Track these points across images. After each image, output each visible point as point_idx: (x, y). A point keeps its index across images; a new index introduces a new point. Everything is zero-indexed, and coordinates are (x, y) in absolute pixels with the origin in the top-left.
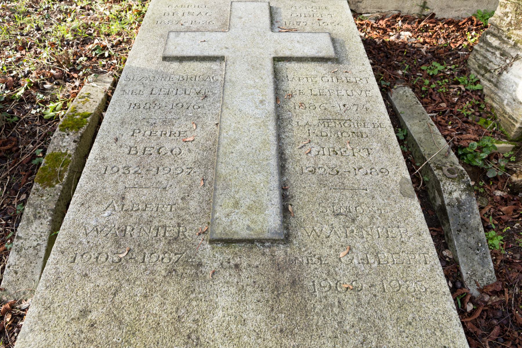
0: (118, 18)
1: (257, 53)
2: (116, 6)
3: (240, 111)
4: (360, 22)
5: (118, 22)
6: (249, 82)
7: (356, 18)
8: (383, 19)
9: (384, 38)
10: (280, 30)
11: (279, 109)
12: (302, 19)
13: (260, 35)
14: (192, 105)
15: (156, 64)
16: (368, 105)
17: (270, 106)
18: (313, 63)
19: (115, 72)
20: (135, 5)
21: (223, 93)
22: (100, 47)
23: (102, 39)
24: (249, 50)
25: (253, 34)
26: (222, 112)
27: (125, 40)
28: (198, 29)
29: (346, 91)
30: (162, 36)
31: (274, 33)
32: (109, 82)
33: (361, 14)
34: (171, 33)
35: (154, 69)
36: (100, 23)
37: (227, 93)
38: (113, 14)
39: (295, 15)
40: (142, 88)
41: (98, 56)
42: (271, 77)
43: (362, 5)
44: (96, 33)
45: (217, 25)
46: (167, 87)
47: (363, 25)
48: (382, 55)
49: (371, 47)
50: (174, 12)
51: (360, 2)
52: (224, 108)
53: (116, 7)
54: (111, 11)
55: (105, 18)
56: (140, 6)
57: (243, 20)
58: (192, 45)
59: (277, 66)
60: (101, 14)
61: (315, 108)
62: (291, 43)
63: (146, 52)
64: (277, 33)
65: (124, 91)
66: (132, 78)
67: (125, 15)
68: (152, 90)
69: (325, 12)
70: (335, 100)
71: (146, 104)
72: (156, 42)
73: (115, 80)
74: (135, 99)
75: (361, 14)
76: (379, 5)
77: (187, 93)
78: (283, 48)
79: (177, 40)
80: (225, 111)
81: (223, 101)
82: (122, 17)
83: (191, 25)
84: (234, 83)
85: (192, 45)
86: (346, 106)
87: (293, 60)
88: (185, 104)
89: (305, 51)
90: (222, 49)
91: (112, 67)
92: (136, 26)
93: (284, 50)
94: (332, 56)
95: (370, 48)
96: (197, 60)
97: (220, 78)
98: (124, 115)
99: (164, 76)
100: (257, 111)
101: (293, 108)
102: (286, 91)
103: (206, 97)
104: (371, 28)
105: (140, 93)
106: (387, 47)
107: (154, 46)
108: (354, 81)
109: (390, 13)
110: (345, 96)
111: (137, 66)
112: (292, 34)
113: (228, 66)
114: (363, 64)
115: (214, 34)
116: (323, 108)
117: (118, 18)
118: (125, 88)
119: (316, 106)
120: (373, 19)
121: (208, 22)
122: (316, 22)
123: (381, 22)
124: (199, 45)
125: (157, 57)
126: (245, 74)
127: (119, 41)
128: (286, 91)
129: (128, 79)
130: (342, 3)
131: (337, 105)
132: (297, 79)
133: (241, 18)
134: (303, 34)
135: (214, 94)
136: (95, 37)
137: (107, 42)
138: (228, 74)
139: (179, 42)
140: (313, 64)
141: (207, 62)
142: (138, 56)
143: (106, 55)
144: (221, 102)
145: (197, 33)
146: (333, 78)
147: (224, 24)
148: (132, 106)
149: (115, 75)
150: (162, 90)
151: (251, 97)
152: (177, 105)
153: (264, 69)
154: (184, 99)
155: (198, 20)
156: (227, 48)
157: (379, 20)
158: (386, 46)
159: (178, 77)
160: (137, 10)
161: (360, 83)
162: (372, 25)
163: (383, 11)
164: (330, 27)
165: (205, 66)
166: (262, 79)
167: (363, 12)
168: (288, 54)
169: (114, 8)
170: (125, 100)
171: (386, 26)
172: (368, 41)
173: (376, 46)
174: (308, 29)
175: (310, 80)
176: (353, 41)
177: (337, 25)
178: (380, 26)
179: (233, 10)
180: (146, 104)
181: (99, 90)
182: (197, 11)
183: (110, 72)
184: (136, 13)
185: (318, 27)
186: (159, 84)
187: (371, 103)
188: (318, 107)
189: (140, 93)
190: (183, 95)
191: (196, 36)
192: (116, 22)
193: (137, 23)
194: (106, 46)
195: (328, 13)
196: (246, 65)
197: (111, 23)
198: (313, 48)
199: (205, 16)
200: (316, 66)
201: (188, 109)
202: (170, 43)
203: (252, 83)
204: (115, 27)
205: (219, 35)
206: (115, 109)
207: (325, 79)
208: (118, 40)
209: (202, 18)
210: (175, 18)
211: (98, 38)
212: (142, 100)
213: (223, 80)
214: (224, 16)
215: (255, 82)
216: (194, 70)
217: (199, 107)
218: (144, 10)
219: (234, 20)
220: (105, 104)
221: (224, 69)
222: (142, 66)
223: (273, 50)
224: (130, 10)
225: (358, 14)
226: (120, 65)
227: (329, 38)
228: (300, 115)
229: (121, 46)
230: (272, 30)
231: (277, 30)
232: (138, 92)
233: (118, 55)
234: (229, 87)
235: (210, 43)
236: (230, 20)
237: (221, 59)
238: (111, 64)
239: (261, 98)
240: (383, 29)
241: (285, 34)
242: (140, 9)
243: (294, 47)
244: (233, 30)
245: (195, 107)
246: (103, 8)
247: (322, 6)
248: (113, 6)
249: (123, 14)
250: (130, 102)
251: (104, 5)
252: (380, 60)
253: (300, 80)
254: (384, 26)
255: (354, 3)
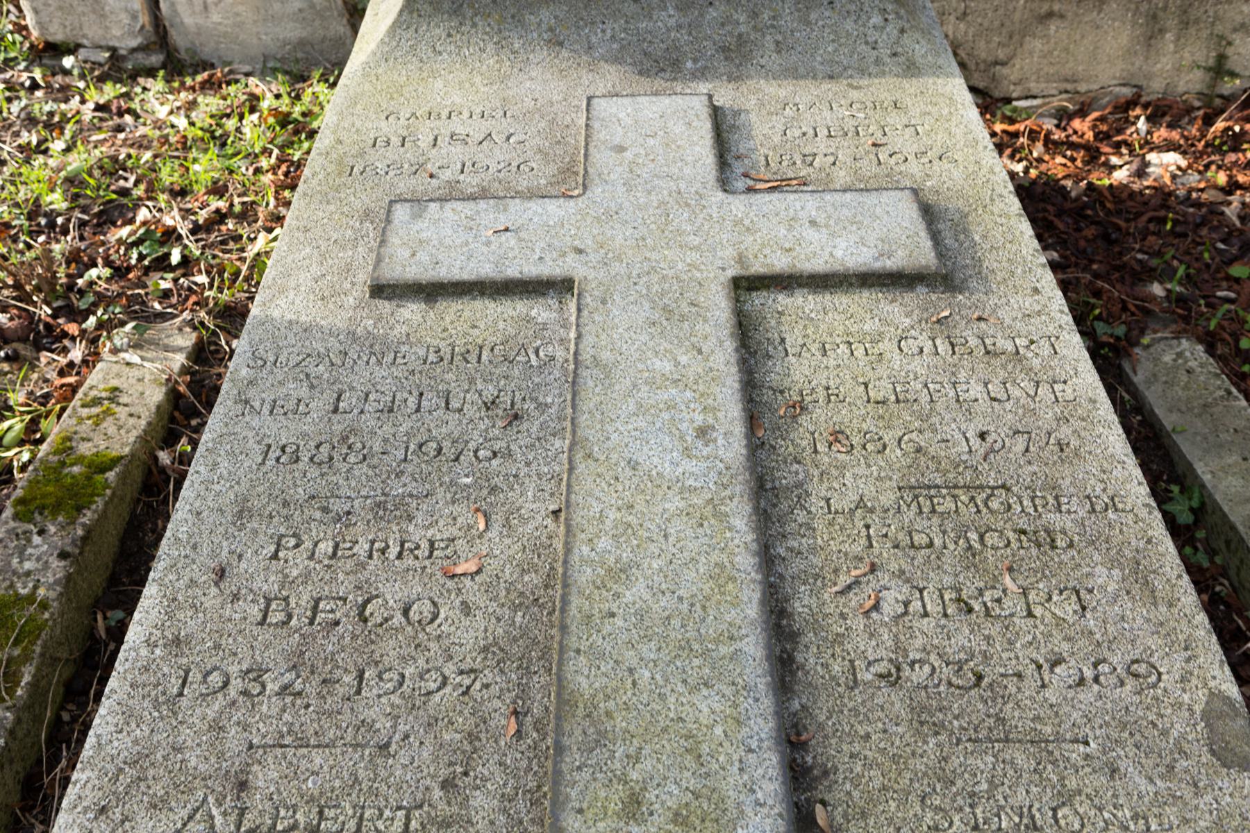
0: (214, 138)
1: (680, 265)
2: (210, 99)
3: (634, 465)
4: (1005, 127)
5: (214, 150)
6: (658, 364)
7: (993, 115)
8: (1082, 113)
9: (1093, 178)
10: (751, 183)
11: (762, 454)
12: (822, 145)
13: (688, 205)
14: (472, 445)
15: (348, 309)
16: (1065, 432)
18: (866, 294)
19: (202, 314)
20: (269, 95)
21: (574, 407)
22: (154, 232)
23: (163, 205)
24: (654, 256)
25: (662, 203)
26: (571, 469)
27: (238, 208)
28: (484, 189)
29: (986, 384)
30: (367, 214)
31: (731, 197)
32: (180, 349)
33: (1008, 101)
34: (398, 206)
36: (155, 156)
38: (199, 125)
39: (797, 133)
40: (304, 392)
41: (146, 263)
42: (730, 345)
43: (1010, 73)
44: (142, 187)
45: (542, 173)
46: (388, 387)
47: (1016, 135)
48: (1090, 232)
49: (1050, 208)
50: (405, 133)
51: (1003, 64)
52: (579, 457)
53: (210, 103)
54: (193, 114)
55: (173, 139)
56: (286, 100)
57: (628, 155)
59: (747, 307)
60: (158, 124)
62: (791, 228)
63: (316, 270)
64: (743, 197)
65: (247, 402)
66: (272, 359)
67: (238, 130)
68: (338, 399)
69: (894, 119)
71: (317, 447)
73: (200, 341)
74: (282, 431)
75: (1008, 101)
76: (1067, 71)
77: (455, 404)
78: (763, 245)
79: (416, 228)
80: (581, 468)
81: (574, 432)
82: (226, 135)
83: (461, 178)
84: (607, 370)
85: (467, 243)
86: (989, 439)
87: (800, 286)
88: (446, 444)
89: (839, 253)
90: (564, 254)
91: (193, 299)
92: (273, 160)
93: (767, 251)
94: (927, 267)
95: (1045, 210)
96: (482, 294)
97: (560, 354)
98: (245, 484)
99: (379, 349)
100: (688, 466)
101: (809, 450)
102: (782, 392)
103: (516, 417)
104: (1045, 145)
105: (298, 410)
106: (1104, 206)
107: (343, 248)
108: (1010, 347)
109: (1105, 95)
110: (984, 405)
111: (289, 316)
112: (792, 196)
113: (585, 313)
115: (535, 206)
116: (910, 448)
117: (214, 138)
118: (251, 393)
119: (886, 439)
120: (1051, 116)
121: (515, 164)
122: (867, 153)
123: (1077, 124)
124: (488, 244)
125: (353, 284)
126: (644, 337)
127: (218, 211)
128: (782, 392)
129: (257, 361)
130: (949, 88)
131: (957, 436)
132: (814, 348)
134: (828, 197)
136: (140, 199)
137: (178, 218)
138: (588, 340)
139: (424, 235)
140: (866, 296)
141: (516, 298)
142: (292, 284)
143: (175, 258)
144: (568, 435)
145: (482, 204)
146: (938, 342)
147: (568, 171)
148: (273, 454)
149: (202, 323)
150: (371, 397)
151: (666, 416)
152: (421, 446)
153: (706, 321)
154: (445, 427)
155: (482, 160)
156: (580, 251)
157: (1071, 117)
158: (1102, 205)
159: (422, 352)
160: (274, 112)
161: (1030, 355)
162: (1049, 133)
163: (1083, 87)
164: (914, 167)
165: (511, 312)
166: (700, 352)
167: (1014, 95)
168: (780, 263)
169: (202, 108)
170: (251, 434)
171: (1096, 136)
172: (1039, 189)
173: (1068, 205)
174: (842, 176)
176: (996, 211)
178: (1074, 138)
179: (596, 125)
180: (317, 447)
181: (148, 377)
182: (477, 129)
183: (186, 315)
184: (271, 120)
185: (875, 169)
186: (360, 378)
188: (892, 444)
189: (298, 410)
190: (441, 412)
191: (478, 212)
192: (206, 151)
193: (276, 152)
194: (175, 229)
195: (905, 121)
196: (647, 306)
197: (194, 153)
198: (863, 242)
199: (505, 145)
200: (878, 301)
201: (457, 459)
202: (394, 240)
203: (668, 366)
204: (204, 167)
205: (554, 209)
206: (215, 464)
207: (910, 346)
208: (213, 208)
209: (497, 151)
210: (409, 154)
211: (150, 204)
212: (304, 435)
213: (571, 358)
217: (495, 454)
218: (297, 110)
219: (601, 158)
220: (165, 421)
221: (573, 319)
222: (303, 318)
223: (730, 252)
224: (253, 110)
225: (998, 100)
226: (220, 290)
227: (915, 206)
228: (834, 472)
229: (223, 228)
230: (724, 184)
231: (740, 184)
232: (291, 405)
233: (214, 257)
234: (591, 383)
235: (523, 235)
236: (586, 156)
237: (561, 287)
238: (190, 289)
239: (699, 419)
240: (1086, 147)
241: (767, 197)
242: (284, 109)
244: (596, 191)
245: (481, 453)
246: (167, 108)
247: (882, 97)
248: (200, 99)
249: (231, 124)
250: (266, 441)
251: (171, 97)
252: (1084, 251)
253: (825, 353)
254: (1090, 135)
255: (982, 67)
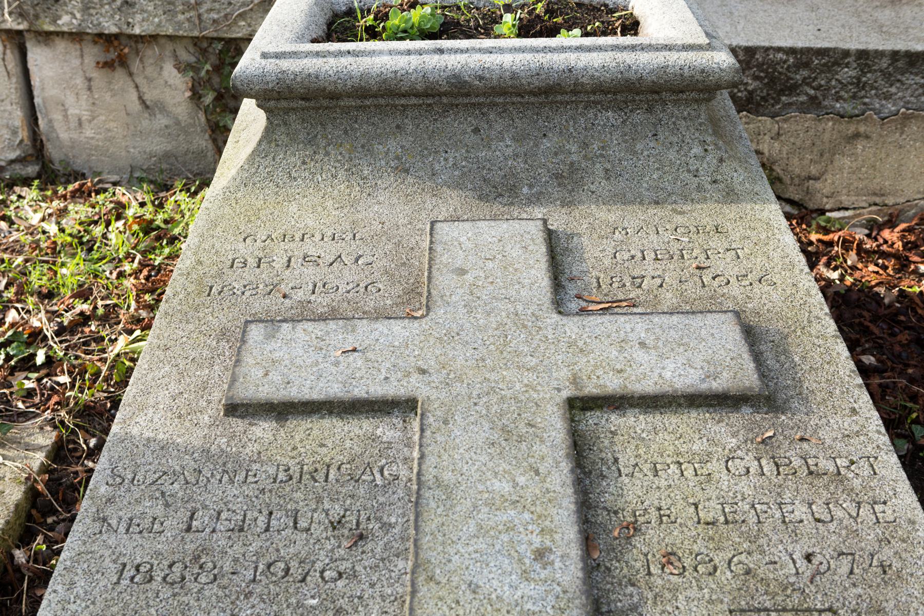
0: (81, 243)
1: (518, 386)
2: (80, 207)
3: (474, 589)
4: (820, 236)
5: (81, 254)
6: (497, 485)
7: (809, 225)
8: (891, 223)
9: (904, 285)
10: (584, 304)
11: (598, 576)
12: (650, 268)
13: (525, 326)
14: (319, 566)
15: (204, 428)
16: (887, 554)
17: (568, 570)
18: (694, 414)
19: (63, 413)
20: (134, 204)
21: (417, 528)
22: (21, 333)
23: (31, 307)
24: (493, 376)
25: (501, 325)
26: (414, 593)
27: (101, 311)
28: (333, 310)
29: (810, 505)
30: (223, 334)
31: (565, 320)
32: (40, 448)
33: (822, 212)
34: (253, 326)
35: (197, 443)
36: (26, 261)
37: (429, 526)
38: (68, 231)
39: (626, 256)
40: (159, 510)
41: (13, 363)
42: (566, 466)
43: (823, 187)
44: (13, 290)
45: (387, 295)
46: (239, 505)
47: (830, 244)
48: (904, 337)
49: (865, 313)
50: (261, 255)
51: (816, 179)
52: (421, 579)
53: (80, 210)
54: (63, 222)
55: (43, 245)
56: (150, 207)
57: (469, 277)
58: (317, 363)
59: (582, 426)
60: (31, 231)
61: (715, 568)
62: (621, 350)
63: (174, 388)
64: (576, 319)
65: (104, 520)
66: (130, 477)
67: (104, 236)
68: (192, 518)
69: (716, 243)
70: (775, 538)
71: (170, 566)
72: (206, 353)
73: (60, 439)
74: (136, 549)
75: (822, 212)
76: (875, 185)
77: (303, 524)
78: (596, 367)
79: (269, 348)
80: (423, 590)
81: (417, 554)
82: (93, 241)
83: (313, 298)
84: (448, 490)
85: (317, 363)
86: (815, 561)
87: (632, 406)
88: (294, 564)
89: (668, 375)
90: (408, 375)
91: (55, 399)
92: (135, 265)
93: (600, 372)
94: (751, 389)
95: (861, 316)
96: (331, 413)
97: (404, 473)
98: (100, 604)
99: (231, 467)
100: (527, 589)
101: (643, 573)
102: (616, 513)
103: (361, 537)
104: (858, 254)
105: (153, 529)
106: (916, 312)
107: (200, 366)
108: (832, 469)
109: (912, 207)
110: (808, 526)
111: (148, 434)
112: (622, 319)
113: (428, 433)
114: (854, 411)
115: (381, 326)
116: (739, 570)
117: (81, 243)
118: (109, 511)
119: (716, 560)
120: (862, 226)
121: (362, 285)
122: (692, 275)
123: (886, 234)
124: (336, 364)
125: (209, 402)
126: (484, 458)
127: (82, 313)
128: (616, 513)
129: (116, 479)
130: (765, 214)
131: (784, 558)
132: (646, 468)
133: (462, 272)
134: (656, 319)
135: (387, 527)
136: (10, 301)
137: (44, 320)
138: (431, 460)
139: (277, 355)
140: (694, 416)
141: (362, 417)
142: (151, 401)
143: (40, 358)
144: (411, 556)
145: (332, 325)
146: (764, 462)
147: (413, 292)
148: (127, 574)
149: (62, 422)
150: (224, 516)
151: (505, 537)
152: (269, 566)
153: (542, 441)
154: (292, 547)
155: (333, 281)
156: (423, 372)
157: (881, 227)
158: (914, 310)
159: (272, 471)
160: (139, 219)
161: (851, 475)
162: (861, 243)
163: (890, 201)
164: (735, 289)
165: (357, 431)
166: (537, 473)
167: (828, 207)
168: (612, 384)
169: (72, 215)
170: (107, 553)
171: (905, 245)
172: (855, 296)
173: (882, 311)
174: (669, 298)
175: (689, 473)
176: (813, 332)
177: (756, 285)
178: (885, 248)
179: (439, 248)
180: (170, 566)
181: (8, 475)
182: (328, 251)
183: (48, 415)
184: (135, 227)
185: (700, 292)
186: (212, 496)
187: (898, 545)
188: (722, 566)
189: (153, 529)
190: (289, 531)
191: (328, 333)
192: (73, 255)
193: (139, 257)
194: (41, 330)
195: (726, 245)
196: (487, 426)
197: (63, 258)
198: (689, 364)
199: (354, 267)
200: (705, 421)
201: (303, 580)
202: (248, 360)
203: (506, 487)
204: (71, 271)
205: (398, 330)
206: (72, 583)
207: (737, 466)
208: (77, 310)
209: (346, 272)
210: (265, 275)
211: (19, 306)
212: (158, 554)
213: (414, 478)
214: (412, 265)
215: (515, 485)
216: (322, 445)
217: (340, 575)
218: (160, 217)
219: (444, 280)
220: (22, 520)
221: (416, 438)
222: (161, 436)
223: (565, 373)
224: (118, 218)
225: (812, 211)
226: (81, 391)
227: (738, 328)
228: (668, 595)
229: (87, 330)
230: (559, 305)
231: (574, 306)
232: (146, 523)
233: (77, 357)
234: (433, 504)
235: (370, 355)
236: (429, 278)
237: (406, 406)
238: (52, 389)
239: (537, 541)
240: (896, 256)
241: (599, 319)
242: (148, 217)
243: (630, 362)
244: (439, 312)
245: (327, 574)
246: (39, 215)
247: (704, 222)
248: (70, 207)
249: (98, 231)
250: (122, 560)
251: (43, 204)
252: (900, 356)
253: (656, 474)
254: (899, 245)
255: (797, 181)
